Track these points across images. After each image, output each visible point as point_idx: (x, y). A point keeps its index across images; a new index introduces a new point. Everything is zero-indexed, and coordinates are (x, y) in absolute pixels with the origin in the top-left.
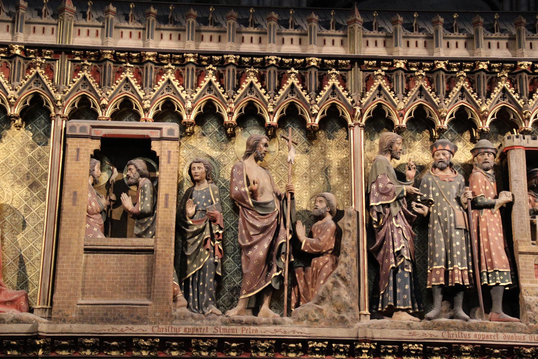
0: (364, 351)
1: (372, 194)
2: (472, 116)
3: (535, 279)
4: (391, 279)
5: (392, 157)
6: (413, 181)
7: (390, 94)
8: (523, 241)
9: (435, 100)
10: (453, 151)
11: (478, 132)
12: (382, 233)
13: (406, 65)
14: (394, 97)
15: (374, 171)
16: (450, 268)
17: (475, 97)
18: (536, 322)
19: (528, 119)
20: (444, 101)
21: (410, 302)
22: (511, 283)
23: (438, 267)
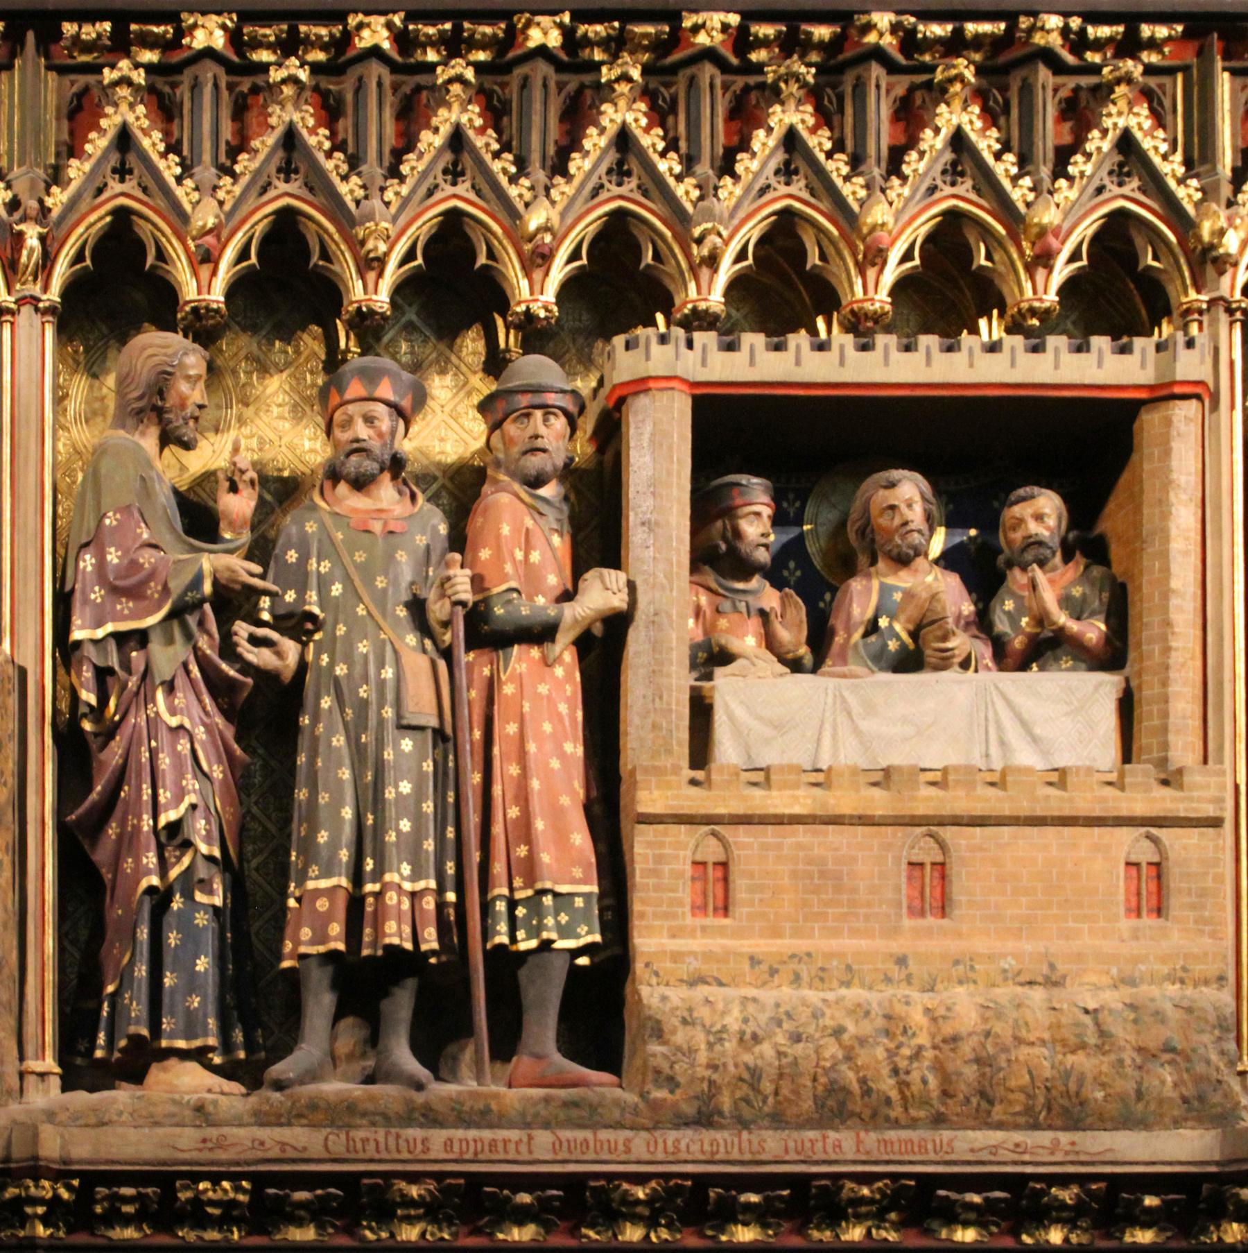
0: (29, 1210)
1: (78, 596)
2: (491, 255)
3: (689, 920)
4: (144, 934)
5: (167, 439)
6: (246, 537)
7: (161, 164)
8: (659, 771)
9: (343, 188)
10: (406, 403)
11: (518, 327)
12: (116, 748)
13: (234, 37)
14: (179, 180)
15: (89, 496)
16: (369, 887)
17: (505, 171)
18: (678, 1085)
19: (712, 261)
20: (382, 189)
21: (212, 1022)
22: (597, 938)
23: (324, 884)
